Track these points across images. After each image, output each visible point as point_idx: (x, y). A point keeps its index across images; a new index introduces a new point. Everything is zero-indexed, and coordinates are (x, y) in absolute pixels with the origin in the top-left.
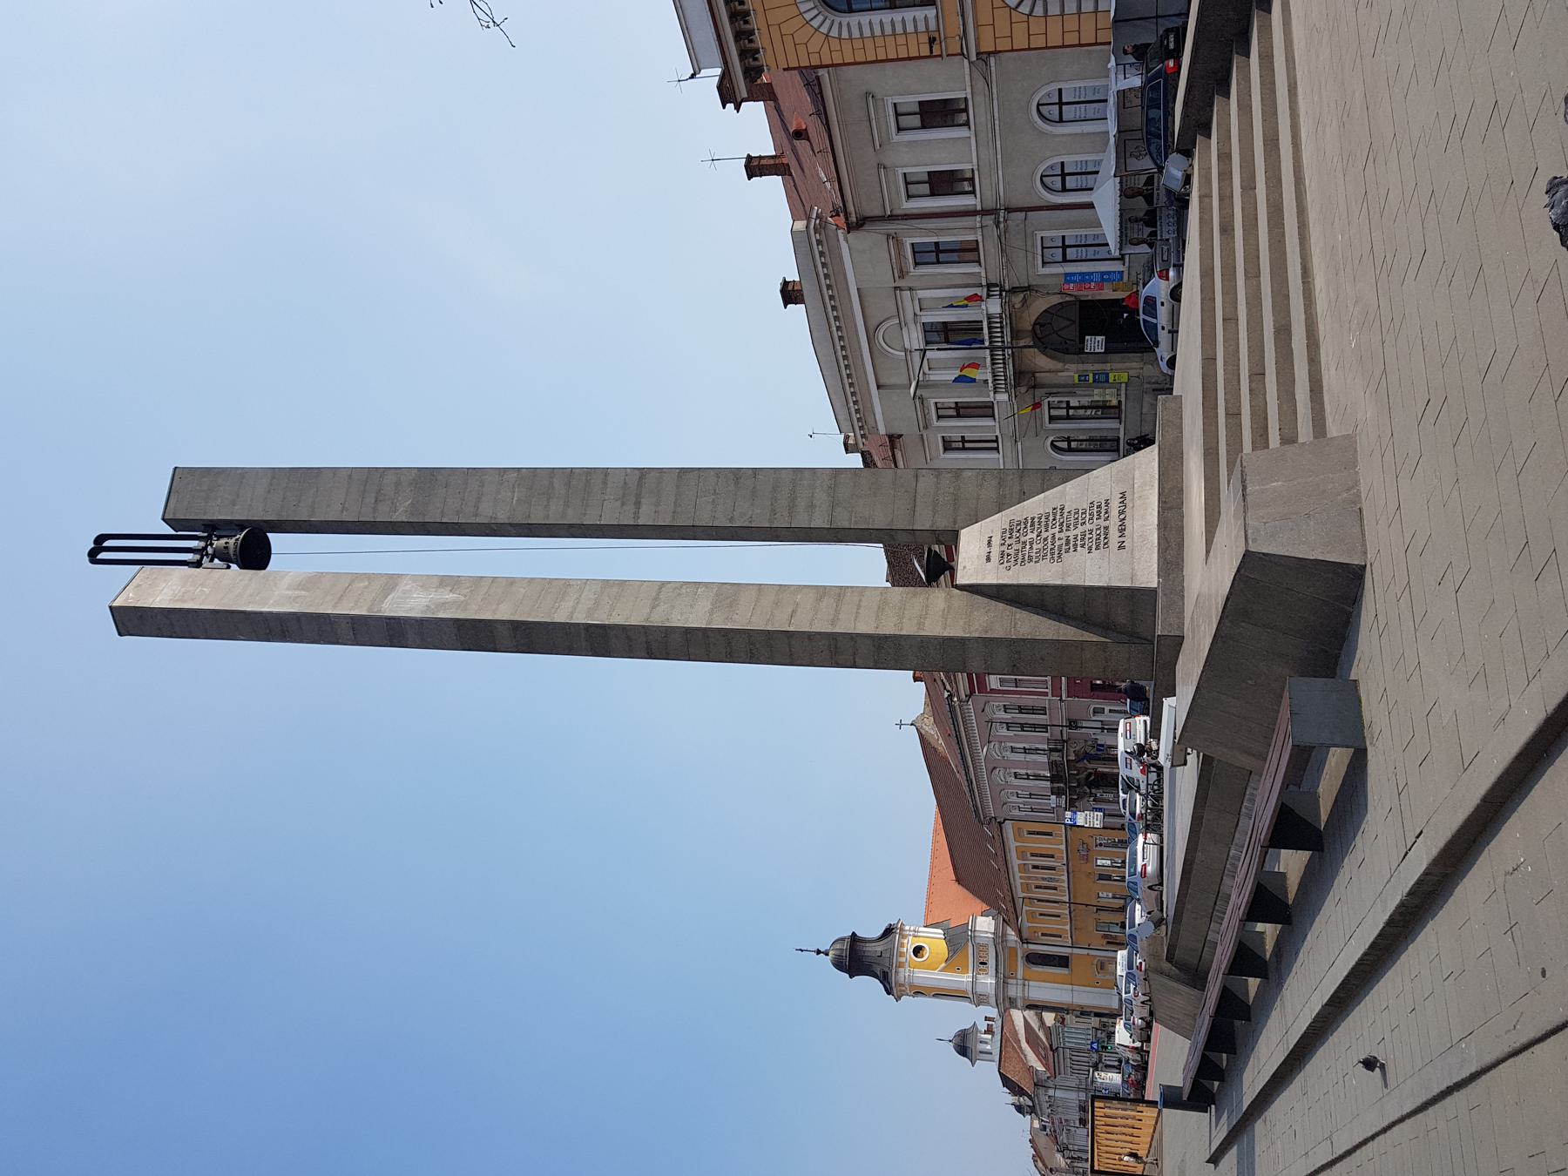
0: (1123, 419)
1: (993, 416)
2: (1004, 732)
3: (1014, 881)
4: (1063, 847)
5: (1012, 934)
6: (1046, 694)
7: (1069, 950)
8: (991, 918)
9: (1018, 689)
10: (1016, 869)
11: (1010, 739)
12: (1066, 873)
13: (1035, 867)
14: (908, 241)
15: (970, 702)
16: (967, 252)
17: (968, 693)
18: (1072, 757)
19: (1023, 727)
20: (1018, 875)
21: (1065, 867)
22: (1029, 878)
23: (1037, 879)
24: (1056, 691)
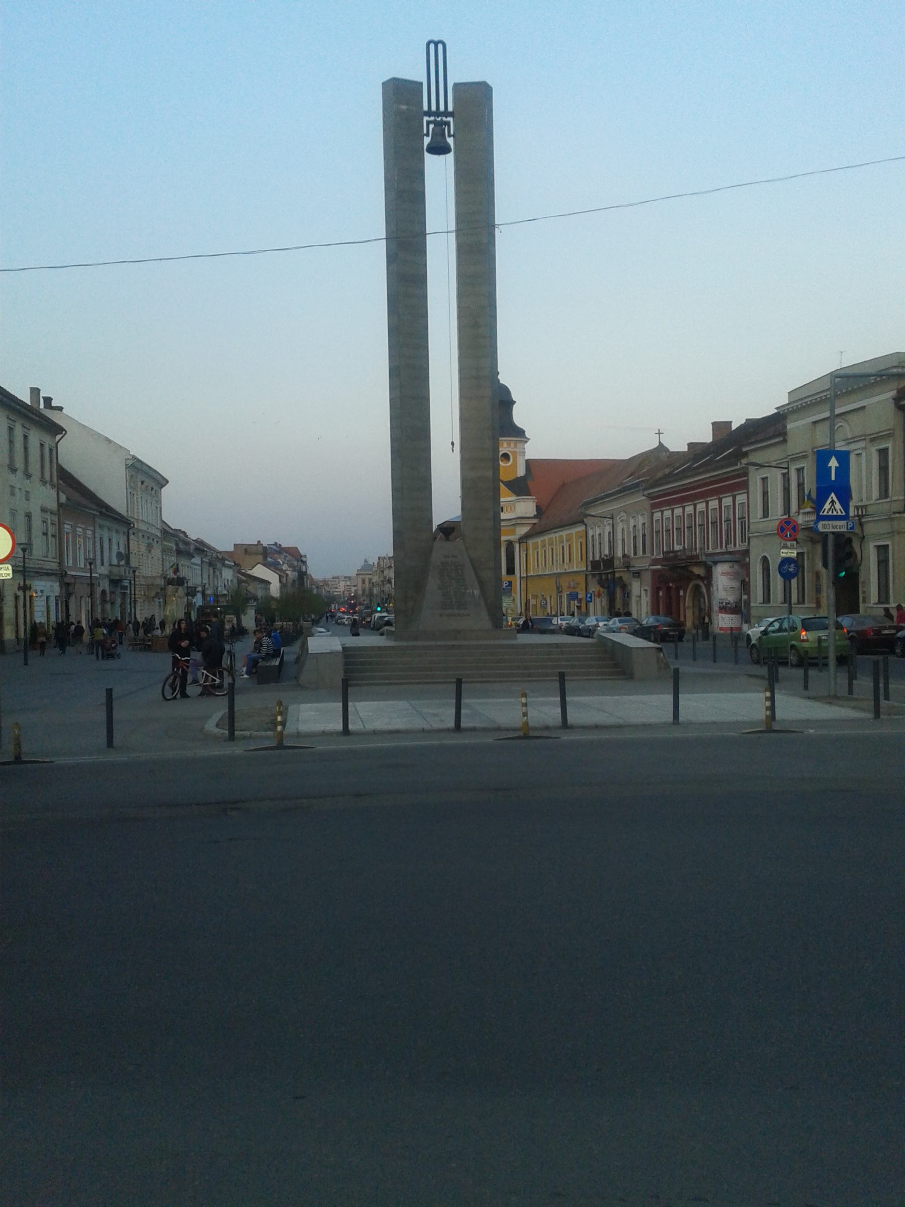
0: (797, 606)
1: (880, 498)
2: (632, 524)
3: (554, 532)
4: (575, 569)
5: (523, 530)
6: (653, 555)
7: (518, 575)
8: (536, 513)
9: (655, 533)
10: (561, 533)
11: (628, 528)
12: (550, 573)
13: (563, 547)
14: (889, 445)
15: (645, 498)
16: (884, 493)
17: (650, 496)
18: (617, 575)
19: (635, 538)
20: (557, 535)
21: (564, 571)
22: (556, 545)
23: (556, 549)
24: (655, 562)
